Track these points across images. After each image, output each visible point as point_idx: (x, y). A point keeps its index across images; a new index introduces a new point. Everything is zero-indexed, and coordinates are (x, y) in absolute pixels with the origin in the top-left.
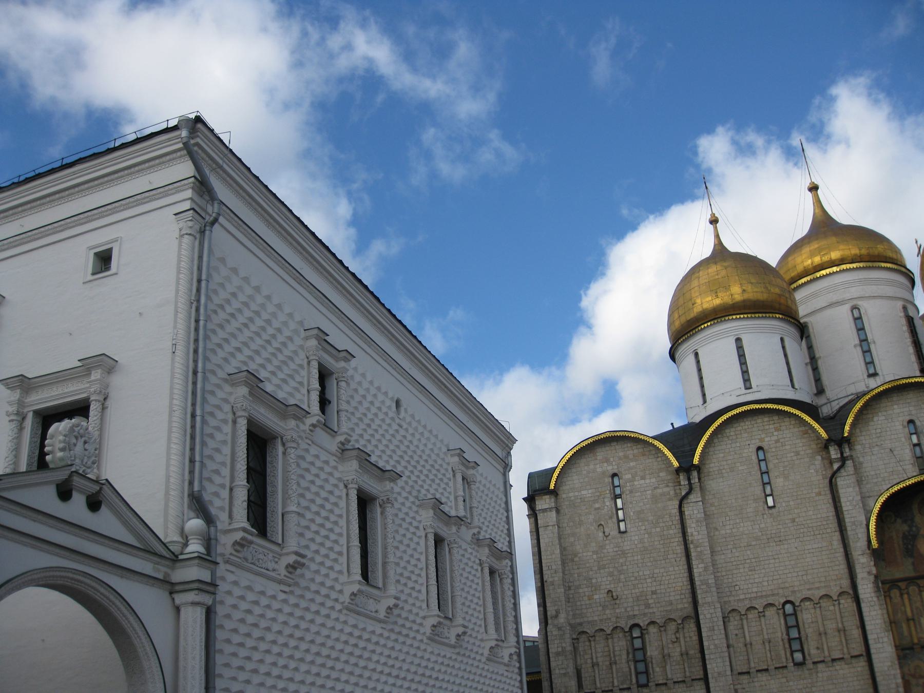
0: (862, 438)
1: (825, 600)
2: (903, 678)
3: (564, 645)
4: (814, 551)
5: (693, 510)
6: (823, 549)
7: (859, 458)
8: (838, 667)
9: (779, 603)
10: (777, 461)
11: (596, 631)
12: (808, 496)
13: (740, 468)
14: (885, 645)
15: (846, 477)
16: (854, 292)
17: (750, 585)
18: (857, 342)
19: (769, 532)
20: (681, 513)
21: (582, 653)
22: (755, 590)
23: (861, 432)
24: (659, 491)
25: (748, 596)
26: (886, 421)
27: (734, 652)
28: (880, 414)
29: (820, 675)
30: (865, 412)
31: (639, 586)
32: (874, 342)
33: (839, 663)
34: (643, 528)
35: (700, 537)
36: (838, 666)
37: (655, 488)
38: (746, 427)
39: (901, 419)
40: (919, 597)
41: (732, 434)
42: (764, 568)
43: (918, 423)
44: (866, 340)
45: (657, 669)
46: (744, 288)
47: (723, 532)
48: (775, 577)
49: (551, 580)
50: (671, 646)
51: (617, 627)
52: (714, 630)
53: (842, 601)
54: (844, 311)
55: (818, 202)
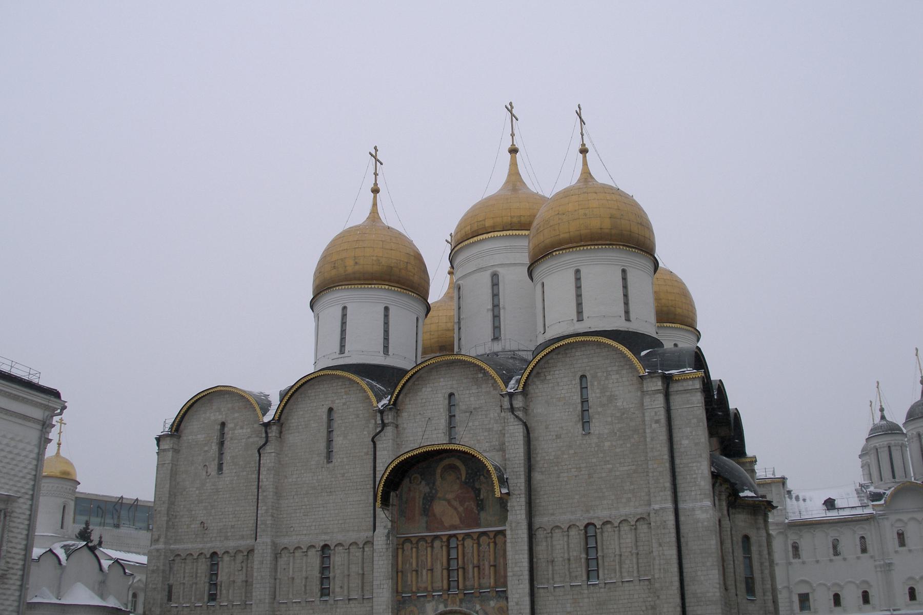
0: (410, 406)
1: (355, 547)
3: (158, 564)
4: (354, 503)
5: (268, 459)
6: (361, 502)
7: (403, 424)
8: (353, 605)
9: (319, 545)
10: (341, 422)
11: (188, 555)
13: (313, 425)
14: (385, 590)
15: (385, 442)
17: (302, 528)
18: (490, 306)
19: (323, 484)
20: (260, 460)
21: (175, 573)
23: (410, 401)
24: (251, 440)
27: (280, 584)
28: (428, 385)
29: (338, 610)
30: (416, 383)
31: (224, 520)
32: (504, 308)
33: (354, 602)
34: (235, 471)
35: (267, 483)
36: (352, 604)
37: (249, 437)
38: (324, 389)
39: (444, 391)
40: (425, 551)
41: (313, 394)
42: (314, 515)
43: (457, 396)
44: (498, 306)
45: (224, 592)
46: (356, 260)
47: (290, 480)
49: (159, 509)
50: (237, 573)
51: (202, 553)
52: (263, 563)
53: (366, 549)
55: (514, 164)
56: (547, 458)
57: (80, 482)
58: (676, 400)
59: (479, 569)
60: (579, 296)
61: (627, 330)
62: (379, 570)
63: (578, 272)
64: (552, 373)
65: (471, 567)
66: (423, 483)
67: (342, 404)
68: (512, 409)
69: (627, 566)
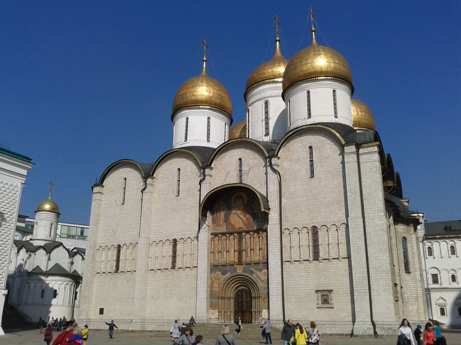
2: (211, 279)
6: (194, 216)
9: (171, 240)
12: (192, 192)
16: (268, 93)
18: (264, 118)
19: (174, 207)
22: (164, 233)
25: (161, 235)
26: (230, 159)
27: (151, 260)
39: (236, 157)
40: (226, 241)
43: (243, 160)
48: (173, 228)
50: (129, 255)
54: (262, 103)
56: (290, 191)
57: (60, 213)
58: (362, 158)
59: (254, 251)
60: (309, 105)
61: (335, 122)
62: (201, 252)
63: (308, 92)
64: (293, 146)
65: (249, 250)
66: (225, 206)
67: (184, 166)
68: (271, 165)
69: (335, 250)
